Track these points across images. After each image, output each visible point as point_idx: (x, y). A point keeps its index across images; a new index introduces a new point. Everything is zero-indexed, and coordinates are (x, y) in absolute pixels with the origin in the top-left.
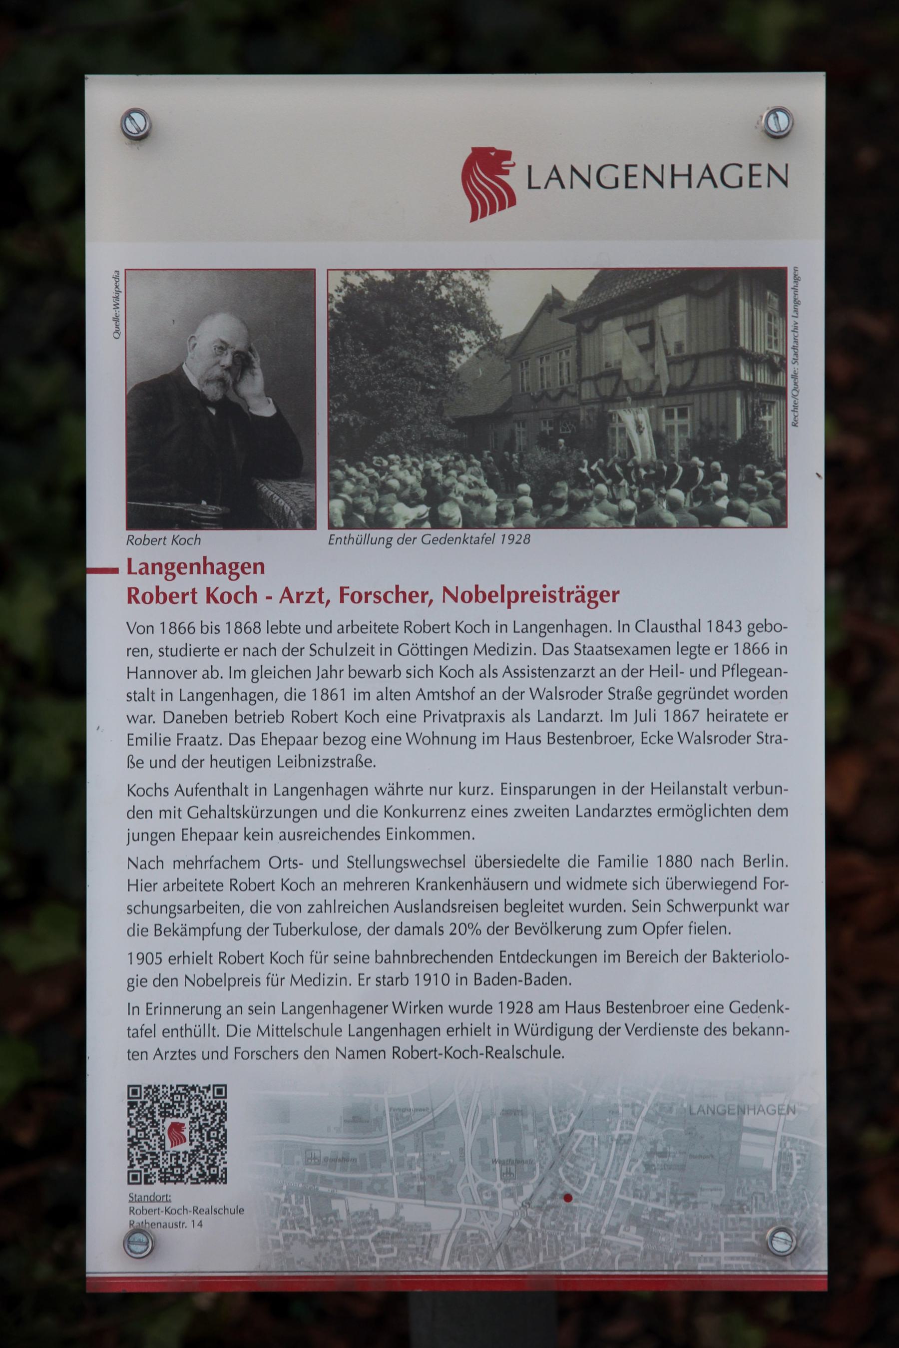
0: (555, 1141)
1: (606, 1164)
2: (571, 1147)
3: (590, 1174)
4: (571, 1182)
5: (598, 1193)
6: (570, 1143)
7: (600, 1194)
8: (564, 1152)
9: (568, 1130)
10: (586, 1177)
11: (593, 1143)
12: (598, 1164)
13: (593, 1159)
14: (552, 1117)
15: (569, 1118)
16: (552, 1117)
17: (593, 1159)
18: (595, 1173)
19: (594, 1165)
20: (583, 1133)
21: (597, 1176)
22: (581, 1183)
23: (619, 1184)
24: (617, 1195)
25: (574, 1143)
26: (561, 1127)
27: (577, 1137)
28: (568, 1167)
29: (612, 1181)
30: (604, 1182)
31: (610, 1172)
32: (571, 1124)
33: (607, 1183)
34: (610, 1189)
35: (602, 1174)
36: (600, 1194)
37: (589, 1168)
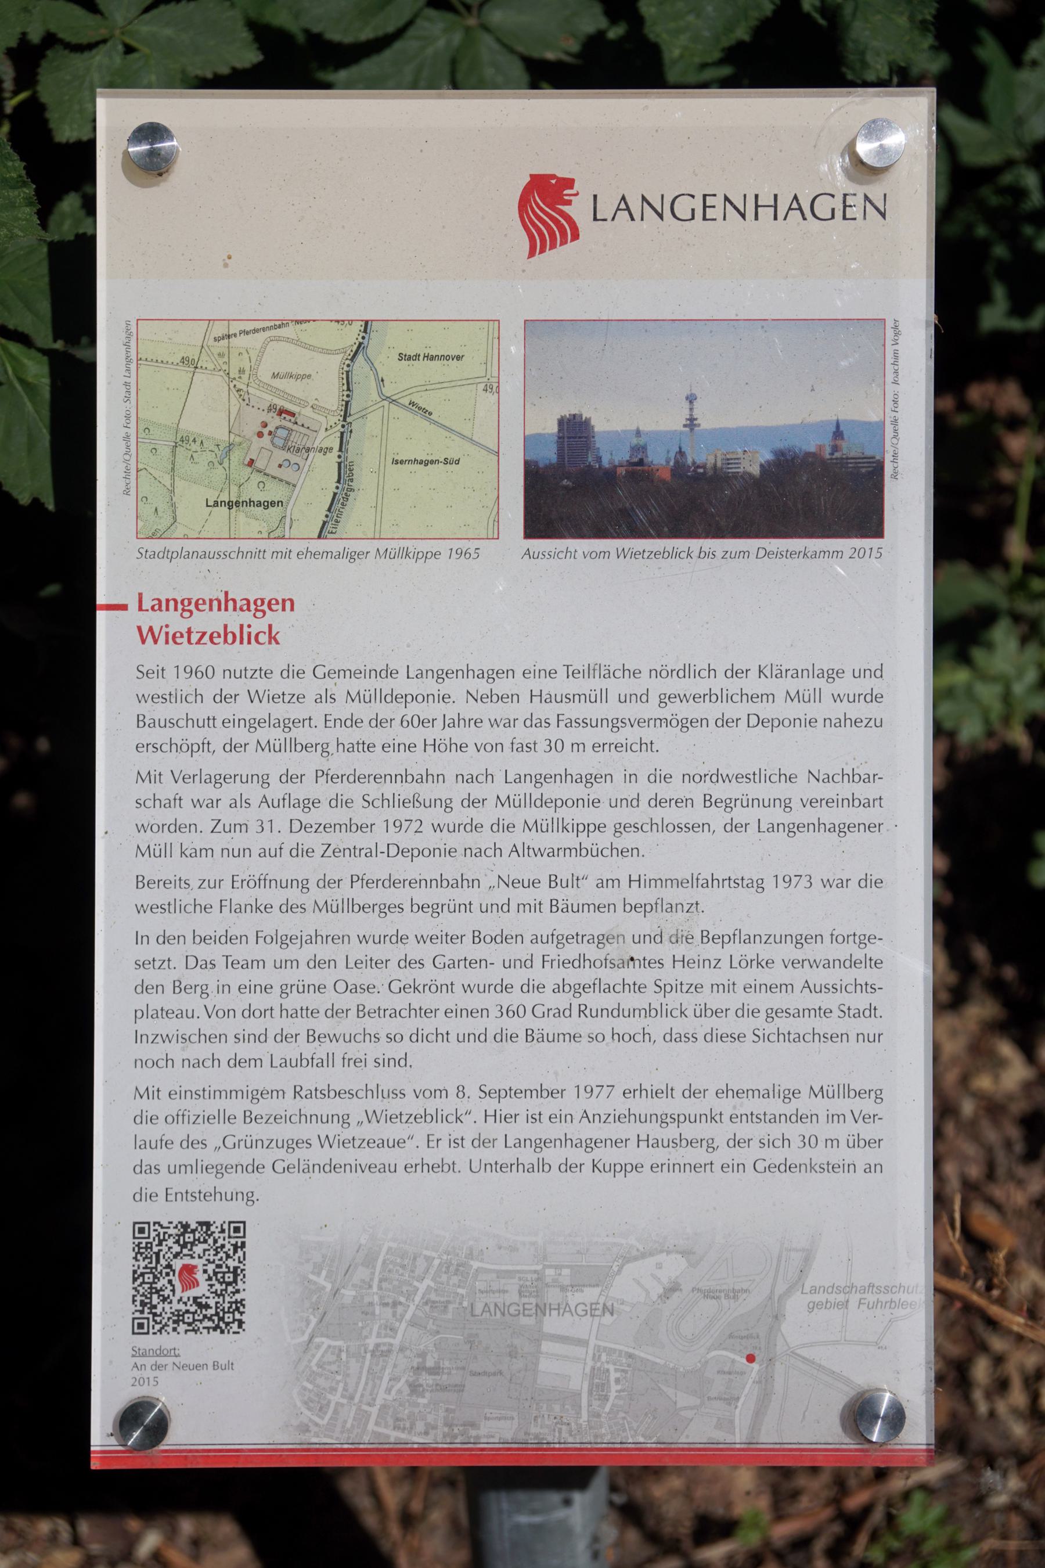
1: (358, 1383)
2: (310, 1361)
3: (336, 1398)
4: (309, 1409)
5: (345, 1422)
7: (348, 1425)
9: (306, 1337)
10: (329, 1402)
11: (339, 1356)
12: (346, 1384)
13: (339, 1378)
18: (343, 1396)
19: (341, 1385)
20: (327, 1342)
21: (345, 1401)
22: (322, 1410)
23: (374, 1411)
24: (371, 1426)
25: (313, 1356)
27: (318, 1347)
28: (305, 1389)
29: (365, 1407)
30: (354, 1408)
31: (362, 1396)
32: (309, 1330)
33: (359, 1409)
34: (362, 1417)
35: (352, 1398)
36: (348, 1425)
37: (333, 1390)
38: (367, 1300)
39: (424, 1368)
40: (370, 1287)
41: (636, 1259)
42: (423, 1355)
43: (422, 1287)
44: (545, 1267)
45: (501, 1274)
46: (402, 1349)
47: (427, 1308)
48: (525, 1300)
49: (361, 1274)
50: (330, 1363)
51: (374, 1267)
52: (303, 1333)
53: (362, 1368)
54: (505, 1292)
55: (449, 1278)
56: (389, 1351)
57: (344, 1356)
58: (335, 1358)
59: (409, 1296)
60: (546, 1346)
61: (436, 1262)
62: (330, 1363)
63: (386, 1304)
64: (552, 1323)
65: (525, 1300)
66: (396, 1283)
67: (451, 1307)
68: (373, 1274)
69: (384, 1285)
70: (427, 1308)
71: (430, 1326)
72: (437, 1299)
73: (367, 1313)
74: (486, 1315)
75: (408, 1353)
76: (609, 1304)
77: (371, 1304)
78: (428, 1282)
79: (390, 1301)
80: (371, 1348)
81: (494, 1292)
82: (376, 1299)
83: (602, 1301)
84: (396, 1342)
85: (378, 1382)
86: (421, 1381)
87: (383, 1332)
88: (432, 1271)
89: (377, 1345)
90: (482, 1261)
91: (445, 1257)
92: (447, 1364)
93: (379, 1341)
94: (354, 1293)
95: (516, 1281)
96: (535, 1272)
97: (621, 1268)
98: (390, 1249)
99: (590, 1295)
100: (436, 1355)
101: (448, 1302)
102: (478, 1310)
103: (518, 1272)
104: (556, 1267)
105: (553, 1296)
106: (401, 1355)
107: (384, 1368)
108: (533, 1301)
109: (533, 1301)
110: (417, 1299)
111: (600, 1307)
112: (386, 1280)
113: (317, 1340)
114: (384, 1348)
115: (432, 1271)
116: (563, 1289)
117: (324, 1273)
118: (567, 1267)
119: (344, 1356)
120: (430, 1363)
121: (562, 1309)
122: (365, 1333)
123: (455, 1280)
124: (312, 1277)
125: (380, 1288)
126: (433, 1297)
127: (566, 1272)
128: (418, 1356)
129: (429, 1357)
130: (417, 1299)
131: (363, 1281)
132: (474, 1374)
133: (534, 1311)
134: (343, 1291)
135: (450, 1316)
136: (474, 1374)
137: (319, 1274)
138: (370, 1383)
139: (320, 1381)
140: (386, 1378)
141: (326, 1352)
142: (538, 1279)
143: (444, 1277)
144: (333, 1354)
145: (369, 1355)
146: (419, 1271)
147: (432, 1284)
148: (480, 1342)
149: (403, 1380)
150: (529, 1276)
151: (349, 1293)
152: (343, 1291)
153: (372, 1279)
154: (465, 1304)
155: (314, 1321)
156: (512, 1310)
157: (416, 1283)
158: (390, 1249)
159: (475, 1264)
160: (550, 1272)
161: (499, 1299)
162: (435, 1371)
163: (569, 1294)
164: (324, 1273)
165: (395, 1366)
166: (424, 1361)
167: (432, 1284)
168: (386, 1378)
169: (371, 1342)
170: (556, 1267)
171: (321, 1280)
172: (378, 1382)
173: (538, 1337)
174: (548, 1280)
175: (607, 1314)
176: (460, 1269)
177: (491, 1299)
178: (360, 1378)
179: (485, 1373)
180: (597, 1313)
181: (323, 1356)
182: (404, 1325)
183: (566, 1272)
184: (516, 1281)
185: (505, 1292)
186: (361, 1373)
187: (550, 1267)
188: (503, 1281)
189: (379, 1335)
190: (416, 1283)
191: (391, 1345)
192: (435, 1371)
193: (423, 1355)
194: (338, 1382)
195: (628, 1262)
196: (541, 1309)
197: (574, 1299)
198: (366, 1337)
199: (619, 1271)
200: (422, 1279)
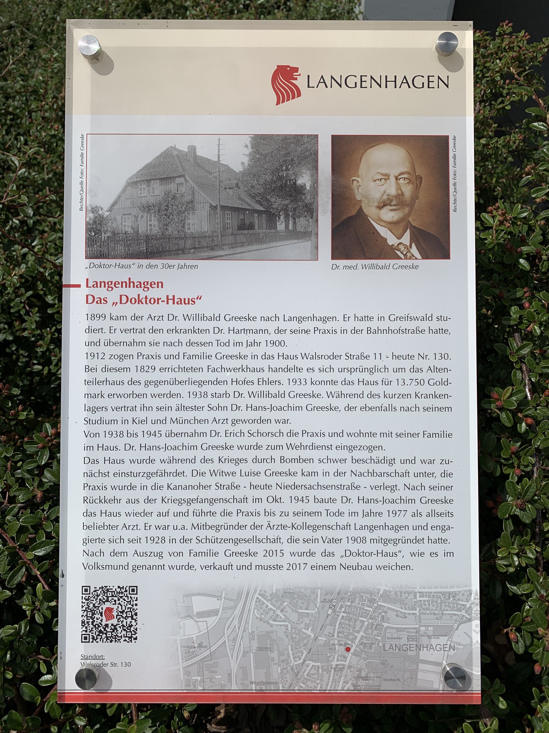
0: (292, 669)
2: (304, 673)
6: (303, 671)
8: (299, 677)
9: (301, 661)
11: (318, 671)
13: (318, 682)
14: (291, 652)
15: (302, 653)
16: (291, 652)
17: (318, 682)
19: (319, 685)
20: (312, 663)
25: (305, 671)
26: (297, 659)
27: (308, 666)
32: (303, 657)
38: (332, 642)
39: (361, 677)
40: (333, 636)
41: (465, 622)
42: (360, 670)
43: (359, 636)
44: (420, 626)
45: (398, 630)
46: (349, 667)
47: (362, 647)
48: (410, 643)
49: (328, 629)
50: (313, 674)
51: (335, 626)
52: (300, 659)
53: (329, 677)
54: (400, 638)
55: (372, 632)
56: (343, 668)
57: (320, 670)
58: (316, 671)
59: (353, 641)
60: (421, 666)
61: (366, 623)
62: (313, 674)
63: (341, 645)
64: (424, 654)
65: (410, 643)
66: (346, 634)
67: (373, 646)
68: (334, 629)
69: (340, 635)
70: (362, 647)
71: (363, 656)
72: (367, 642)
73: (332, 648)
74: (391, 650)
75: (352, 669)
76: (452, 645)
77: (334, 644)
78: (362, 633)
79: (343, 643)
80: (334, 666)
81: (395, 639)
82: (336, 642)
83: (449, 643)
84: (347, 663)
85: (337, 684)
86: (359, 684)
87: (340, 658)
88: (364, 628)
89: (337, 665)
90: (389, 623)
91: (370, 621)
92: (372, 675)
93: (338, 663)
94: (325, 639)
95: (406, 633)
96: (415, 628)
97: (458, 626)
98: (343, 616)
99: (443, 640)
100: (366, 670)
101: (372, 643)
102: (387, 648)
103: (407, 628)
104: (426, 626)
105: (424, 641)
106: (349, 670)
107: (341, 676)
108: (415, 643)
109: (415, 643)
110: (357, 641)
111: (448, 646)
112: (340, 632)
113: (307, 662)
114: (341, 667)
115: (364, 628)
116: (429, 637)
117: (310, 628)
118: (430, 626)
119: (320, 670)
120: (363, 674)
121: (430, 647)
122: (331, 659)
123: (375, 632)
124: (304, 630)
125: (338, 636)
126: (364, 641)
127: (431, 628)
128: (357, 671)
129: (363, 671)
130: (357, 641)
131: (329, 633)
132: (385, 680)
133: (415, 649)
134: (320, 638)
135: (373, 650)
136: (385, 680)
137: (308, 629)
138: (334, 684)
139: (309, 683)
140: (341, 682)
141: (311, 668)
142: (416, 632)
143: (370, 631)
144: (315, 669)
145: (333, 670)
146: (357, 628)
147: (364, 635)
148: (388, 664)
149: (350, 683)
150: (412, 631)
151: (322, 639)
152: (320, 638)
153: (334, 632)
154: (381, 645)
155: (305, 653)
156: (404, 647)
157: (356, 634)
158: (343, 616)
159: (386, 625)
160: (423, 629)
161: (398, 642)
162: (366, 678)
163: (432, 640)
164: (310, 628)
165: (346, 676)
166: (361, 673)
167: (364, 635)
168: (341, 682)
169: (334, 663)
170: (426, 626)
171: (309, 632)
172: (337, 684)
173: (417, 661)
174: (422, 633)
175: (452, 650)
176: (378, 627)
177: (393, 642)
178: (328, 682)
179: (391, 680)
180: (447, 649)
181: (310, 670)
182: (350, 655)
183: (431, 628)
184: (406, 633)
185: (400, 638)
186: (329, 679)
187: (423, 626)
188: (399, 633)
189: (338, 660)
190: (356, 634)
191: (344, 665)
192: (366, 678)
193: (360, 670)
194: (318, 684)
195: (462, 623)
196: (419, 648)
197: (434, 642)
198: (332, 661)
199: (457, 629)
200: (358, 632)
